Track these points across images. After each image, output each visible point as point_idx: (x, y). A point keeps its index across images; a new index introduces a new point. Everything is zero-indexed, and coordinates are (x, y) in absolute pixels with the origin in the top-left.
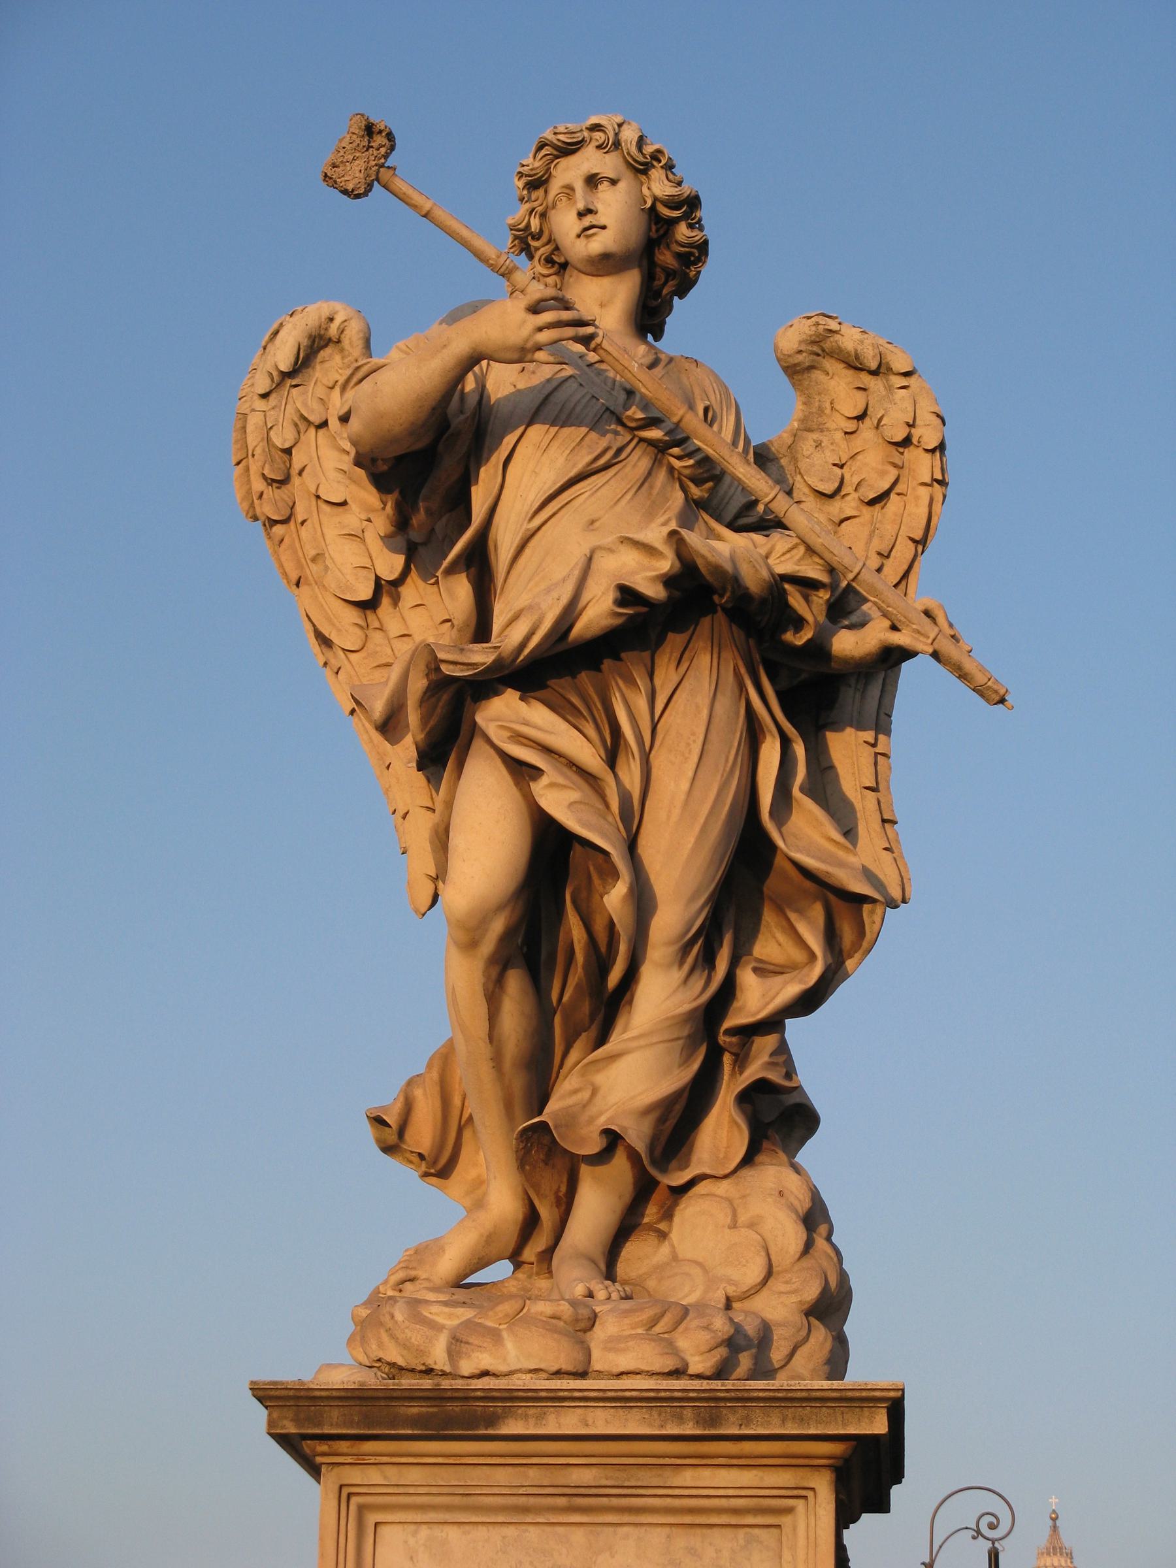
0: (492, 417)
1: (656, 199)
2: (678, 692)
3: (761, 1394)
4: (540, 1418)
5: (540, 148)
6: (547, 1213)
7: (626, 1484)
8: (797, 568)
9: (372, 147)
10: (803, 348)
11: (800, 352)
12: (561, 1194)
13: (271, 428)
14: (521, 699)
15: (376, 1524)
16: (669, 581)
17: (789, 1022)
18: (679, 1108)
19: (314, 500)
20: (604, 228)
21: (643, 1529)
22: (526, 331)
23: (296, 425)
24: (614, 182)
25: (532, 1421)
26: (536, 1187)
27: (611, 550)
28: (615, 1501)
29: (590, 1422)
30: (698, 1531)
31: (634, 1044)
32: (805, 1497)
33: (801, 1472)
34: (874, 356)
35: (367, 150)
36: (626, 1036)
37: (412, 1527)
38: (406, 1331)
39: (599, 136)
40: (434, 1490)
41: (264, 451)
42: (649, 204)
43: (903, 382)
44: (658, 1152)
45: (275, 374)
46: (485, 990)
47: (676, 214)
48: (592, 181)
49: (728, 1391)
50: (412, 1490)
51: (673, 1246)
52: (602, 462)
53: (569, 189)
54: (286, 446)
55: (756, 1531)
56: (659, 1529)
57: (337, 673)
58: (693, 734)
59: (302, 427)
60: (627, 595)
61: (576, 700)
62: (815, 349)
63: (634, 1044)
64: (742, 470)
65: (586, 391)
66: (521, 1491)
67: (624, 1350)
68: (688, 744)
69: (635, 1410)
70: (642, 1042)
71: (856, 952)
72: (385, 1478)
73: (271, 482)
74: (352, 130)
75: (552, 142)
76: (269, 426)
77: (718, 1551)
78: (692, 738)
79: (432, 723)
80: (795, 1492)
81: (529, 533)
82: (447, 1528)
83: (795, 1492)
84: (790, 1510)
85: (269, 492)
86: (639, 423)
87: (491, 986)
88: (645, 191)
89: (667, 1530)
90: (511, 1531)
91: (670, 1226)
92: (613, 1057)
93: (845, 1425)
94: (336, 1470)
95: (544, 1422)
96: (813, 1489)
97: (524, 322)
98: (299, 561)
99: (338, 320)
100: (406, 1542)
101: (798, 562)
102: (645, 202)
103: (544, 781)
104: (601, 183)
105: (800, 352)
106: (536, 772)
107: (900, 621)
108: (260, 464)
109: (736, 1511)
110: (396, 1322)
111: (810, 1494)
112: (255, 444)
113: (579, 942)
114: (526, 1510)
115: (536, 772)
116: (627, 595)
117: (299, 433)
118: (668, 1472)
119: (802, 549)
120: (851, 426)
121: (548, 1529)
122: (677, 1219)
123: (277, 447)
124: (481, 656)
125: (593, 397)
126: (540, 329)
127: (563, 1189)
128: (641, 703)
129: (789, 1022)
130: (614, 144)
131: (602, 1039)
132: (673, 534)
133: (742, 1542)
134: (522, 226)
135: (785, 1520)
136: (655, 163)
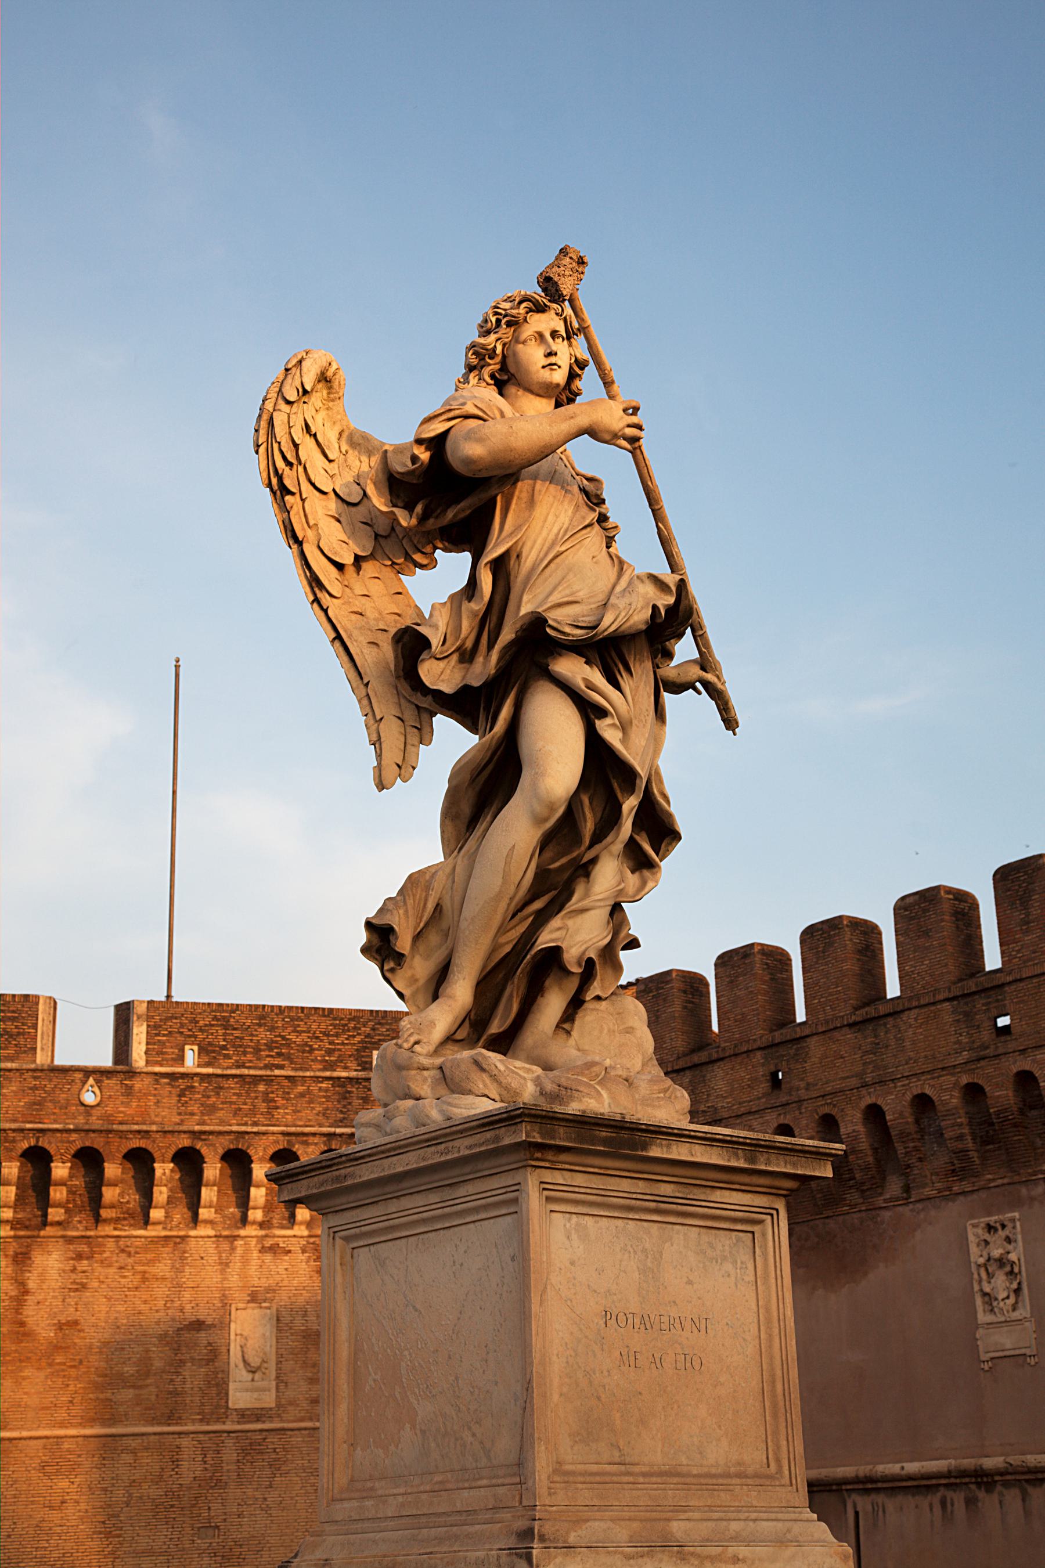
3: (781, 1145)
7: (689, 1197)
21: (686, 1228)
22: (621, 424)
25: (665, 1149)
30: (713, 1231)
31: (599, 904)
33: (771, 1197)
37: (567, 1215)
40: (588, 1191)
49: (765, 1141)
50: (577, 1189)
55: (741, 1234)
56: (694, 1229)
63: (599, 904)
66: (634, 1196)
67: (660, 1106)
69: (715, 1148)
72: (564, 1179)
77: (723, 1246)
79: (501, 664)
82: (587, 1218)
84: (761, 1222)
89: (697, 1229)
90: (620, 1223)
91: (572, 1027)
93: (814, 1170)
94: (538, 1171)
99: (334, 366)
100: (565, 1226)
103: (608, 721)
104: (558, 338)
109: (735, 1220)
110: (500, 1071)
114: (630, 1209)
118: (708, 1191)
121: (639, 1223)
126: (629, 426)
135: (756, 1229)
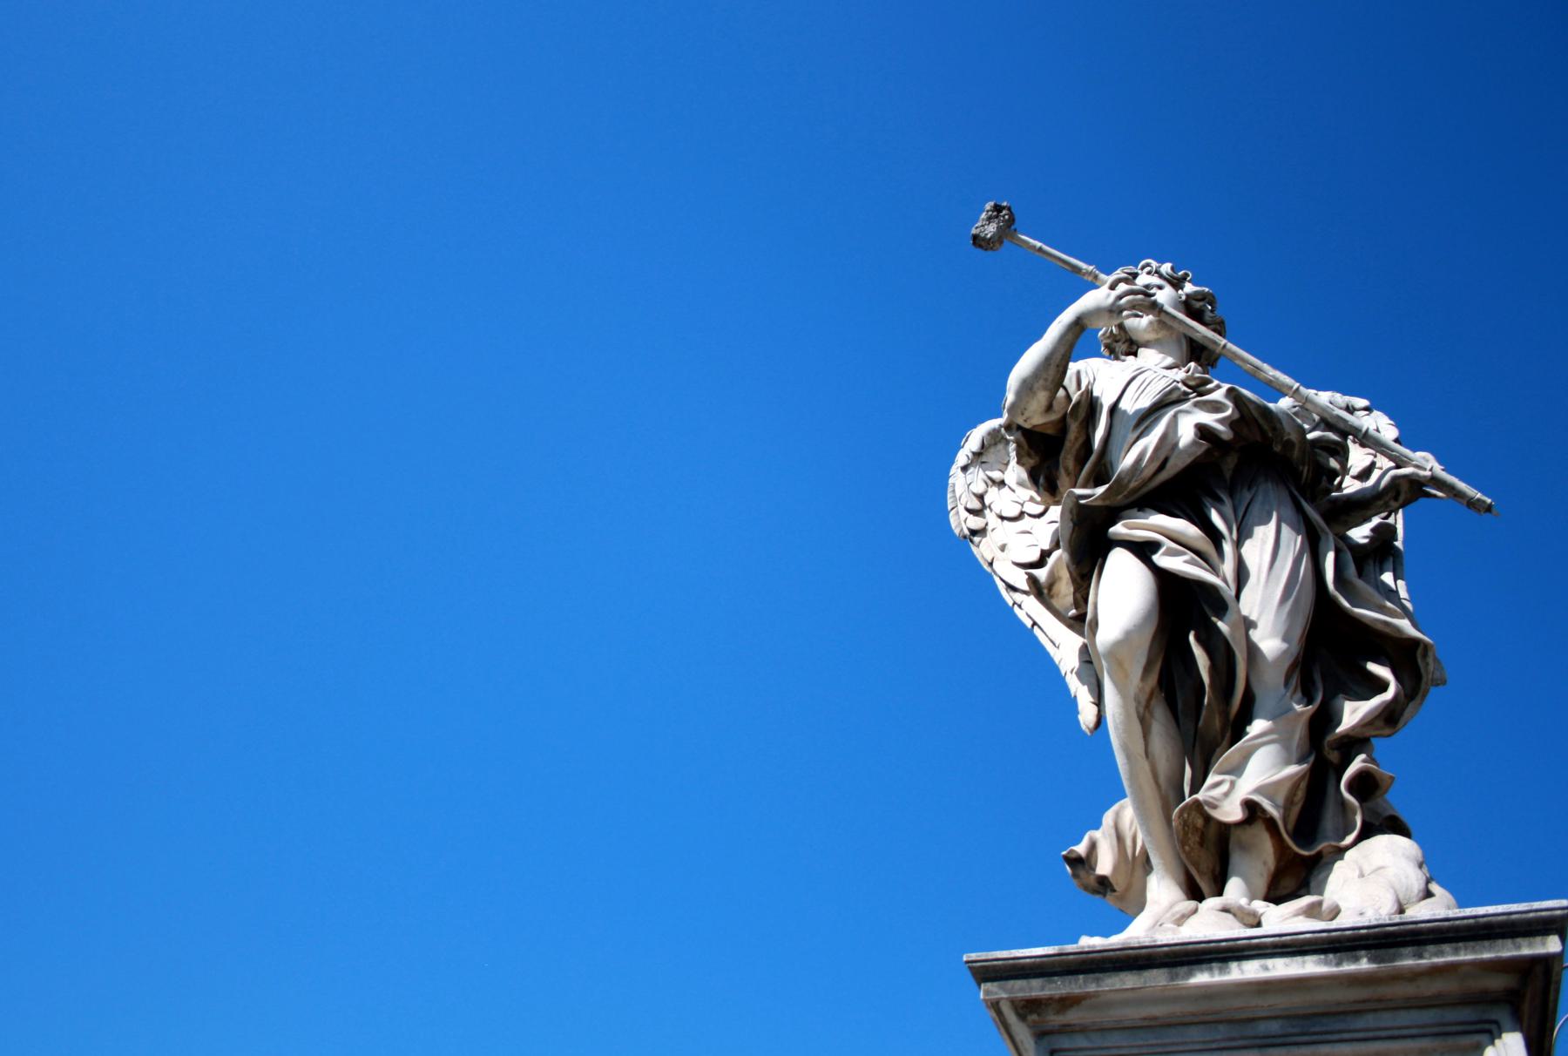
11: (1295, 407)
12: (1217, 873)
14: (1139, 511)
16: (1232, 424)
18: (1300, 794)
22: (1111, 300)
23: (986, 483)
26: (1197, 865)
27: (1187, 412)
44: (1290, 827)
46: (1138, 712)
59: (990, 483)
60: (1203, 431)
64: (1271, 373)
71: (1417, 694)
73: (970, 511)
80: (1479, 1027)
83: (1479, 1027)
87: (1141, 710)
95: (1228, 970)
97: (1109, 295)
105: (1295, 407)
111: (1493, 1027)
115: (1154, 546)
116: (1203, 431)
117: (987, 486)
119: (1322, 425)
127: (1218, 869)
128: (1228, 509)
132: (1230, 391)
134: (1108, 334)
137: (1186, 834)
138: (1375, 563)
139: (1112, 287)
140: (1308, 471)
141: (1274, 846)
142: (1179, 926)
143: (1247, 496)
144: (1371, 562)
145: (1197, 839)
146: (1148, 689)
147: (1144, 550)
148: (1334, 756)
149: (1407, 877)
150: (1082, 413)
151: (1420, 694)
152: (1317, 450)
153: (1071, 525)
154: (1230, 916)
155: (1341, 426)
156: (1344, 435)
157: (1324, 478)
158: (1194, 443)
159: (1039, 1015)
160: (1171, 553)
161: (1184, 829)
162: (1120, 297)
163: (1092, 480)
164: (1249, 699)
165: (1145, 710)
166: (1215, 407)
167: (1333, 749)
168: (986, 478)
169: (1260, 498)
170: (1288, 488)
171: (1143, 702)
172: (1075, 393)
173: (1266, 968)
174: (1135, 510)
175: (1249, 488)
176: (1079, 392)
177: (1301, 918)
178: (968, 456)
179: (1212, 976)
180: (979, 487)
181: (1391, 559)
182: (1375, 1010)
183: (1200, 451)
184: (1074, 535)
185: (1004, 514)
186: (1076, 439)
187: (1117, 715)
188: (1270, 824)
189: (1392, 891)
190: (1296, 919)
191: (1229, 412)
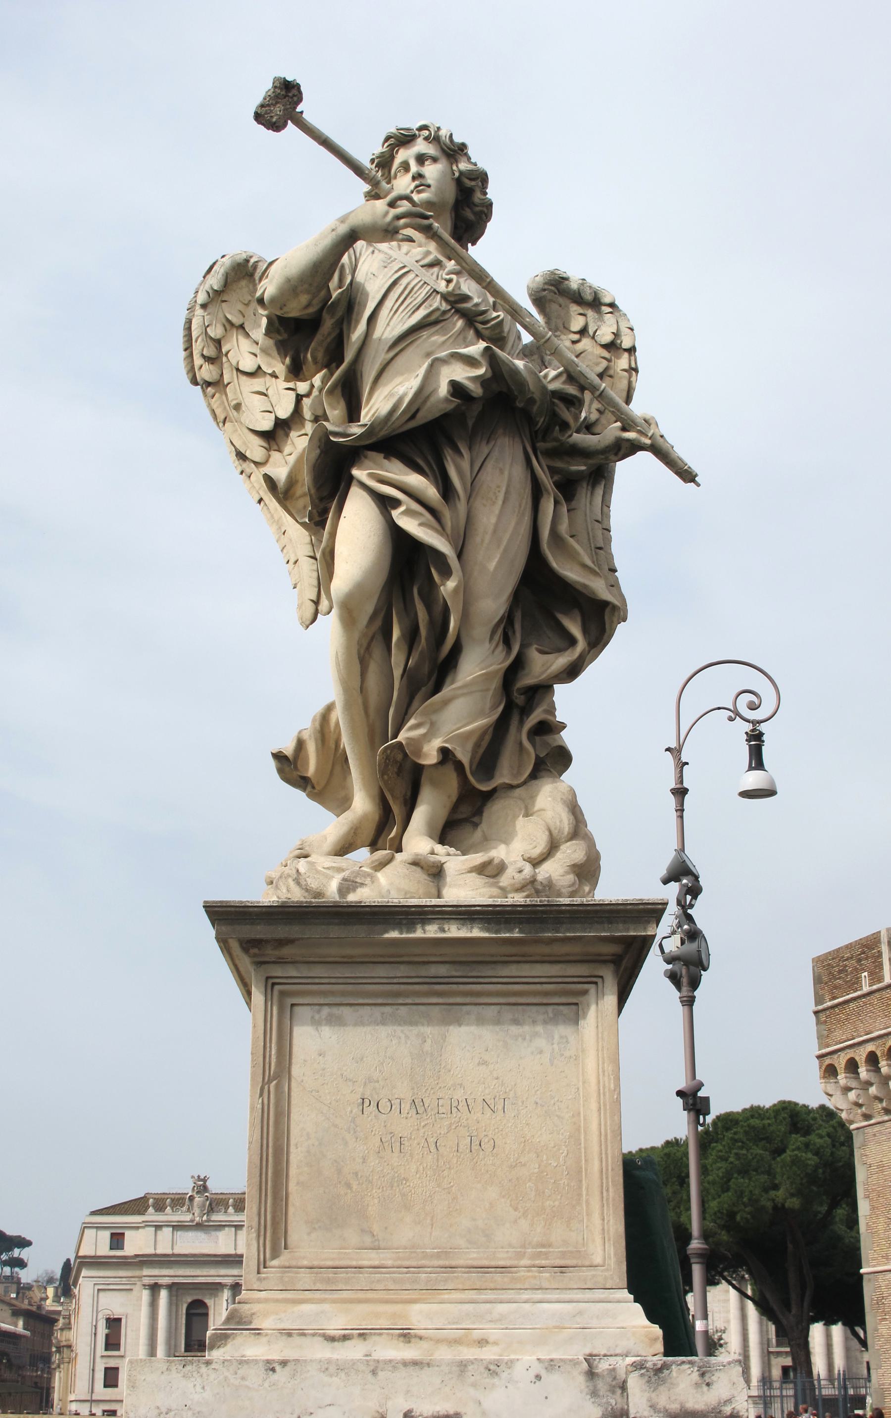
0: (359, 294)
1: (461, 173)
2: (487, 460)
4: (411, 927)
5: (387, 140)
6: (397, 809)
8: (562, 386)
9: (288, 96)
10: (546, 287)
11: (544, 290)
12: (408, 797)
13: (208, 326)
14: (385, 458)
15: (293, 1005)
16: (482, 381)
17: (557, 687)
18: (488, 738)
19: (235, 372)
20: (429, 186)
21: (481, 1007)
22: (389, 218)
23: (224, 326)
24: (435, 160)
28: (462, 987)
29: (446, 929)
30: (520, 1007)
31: (460, 692)
32: (596, 983)
34: (590, 293)
35: (285, 98)
36: (453, 686)
37: (317, 1007)
38: (307, 879)
39: (425, 133)
40: (333, 981)
41: (203, 340)
42: (457, 174)
43: (610, 310)
44: (474, 767)
45: (210, 292)
46: (359, 654)
47: (473, 183)
48: (421, 159)
50: (317, 981)
51: (483, 832)
52: (433, 318)
53: (406, 167)
54: (218, 337)
55: (561, 1008)
57: (250, 477)
58: (498, 487)
59: (228, 327)
60: (456, 388)
61: (421, 462)
62: (553, 288)
63: (460, 692)
64: (528, 320)
65: (420, 279)
66: (395, 981)
68: (495, 493)
70: (465, 691)
74: (275, 84)
75: (395, 134)
76: (206, 324)
78: (498, 489)
80: (589, 979)
81: (385, 362)
82: (342, 1008)
83: (589, 979)
85: (206, 366)
86: (457, 298)
87: (362, 651)
88: (455, 168)
89: (498, 1008)
90: (387, 1009)
91: (481, 820)
92: (446, 702)
96: (602, 977)
97: (387, 213)
98: (225, 408)
101: (564, 383)
102: (454, 174)
103: (402, 509)
104: (427, 160)
105: (544, 290)
106: (396, 503)
107: (629, 424)
108: (201, 347)
109: (546, 994)
111: (599, 980)
112: (197, 336)
113: (423, 621)
114: (398, 994)
115: (396, 503)
116: (456, 388)
120: (576, 337)
121: (415, 1007)
122: (485, 814)
123: (211, 338)
124: (356, 430)
125: (425, 283)
127: (409, 794)
128: (465, 464)
129: (557, 687)
130: (434, 138)
131: (437, 689)
132: (487, 349)
133: (551, 1015)
136: (460, 152)
137: (386, 765)
138: (588, 485)
139: (392, 204)
140: (543, 422)
141: (458, 783)
142: (376, 871)
143: (485, 450)
144: (585, 485)
145: (396, 770)
146: (370, 634)
147: (385, 503)
148: (520, 700)
149: (561, 821)
150: (340, 313)
151: (602, 643)
152: (556, 401)
153: (318, 451)
154: (418, 869)
155: (582, 381)
156: (582, 388)
157: (557, 428)
158: (446, 400)
159: (259, 949)
160: (408, 512)
161: (385, 762)
162: (398, 217)
163: (340, 385)
164: (457, 650)
165: (365, 652)
166: (470, 361)
167: (521, 694)
168: (224, 321)
169: (495, 454)
170: (523, 442)
171: (365, 645)
172: (335, 290)
173: (443, 931)
174: (382, 455)
175: (488, 442)
176: (340, 290)
177: (474, 874)
178: (208, 293)
179: (401, 934)
180: (216, 332)
181: (603, 483)
182: (519, 962)
183: (450, 407)
184: (319, 461)
185: (241, 368)
186: (329, 334)
187: (339, 654)
188: (459, 766)
189: (547, 833)
190: (469, 875)
191: (481, 371)
